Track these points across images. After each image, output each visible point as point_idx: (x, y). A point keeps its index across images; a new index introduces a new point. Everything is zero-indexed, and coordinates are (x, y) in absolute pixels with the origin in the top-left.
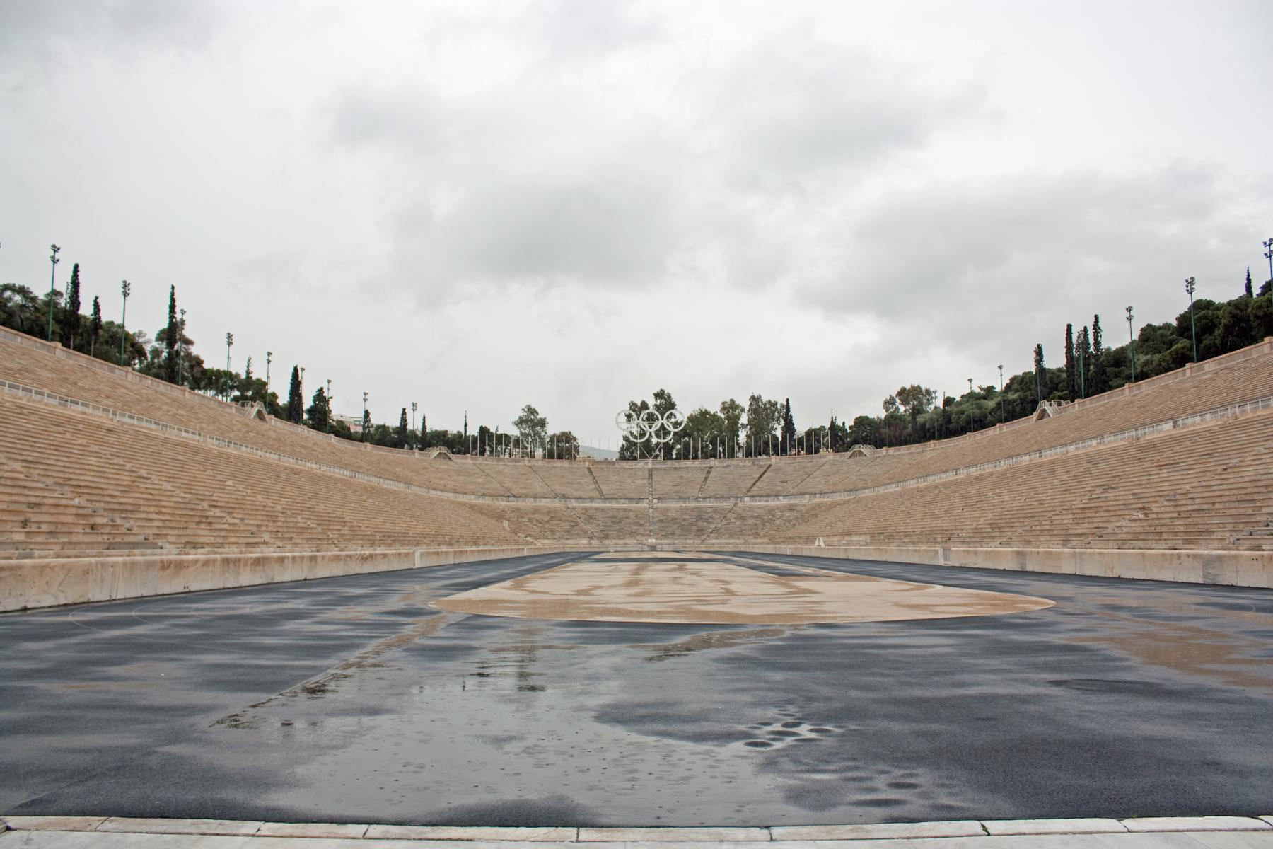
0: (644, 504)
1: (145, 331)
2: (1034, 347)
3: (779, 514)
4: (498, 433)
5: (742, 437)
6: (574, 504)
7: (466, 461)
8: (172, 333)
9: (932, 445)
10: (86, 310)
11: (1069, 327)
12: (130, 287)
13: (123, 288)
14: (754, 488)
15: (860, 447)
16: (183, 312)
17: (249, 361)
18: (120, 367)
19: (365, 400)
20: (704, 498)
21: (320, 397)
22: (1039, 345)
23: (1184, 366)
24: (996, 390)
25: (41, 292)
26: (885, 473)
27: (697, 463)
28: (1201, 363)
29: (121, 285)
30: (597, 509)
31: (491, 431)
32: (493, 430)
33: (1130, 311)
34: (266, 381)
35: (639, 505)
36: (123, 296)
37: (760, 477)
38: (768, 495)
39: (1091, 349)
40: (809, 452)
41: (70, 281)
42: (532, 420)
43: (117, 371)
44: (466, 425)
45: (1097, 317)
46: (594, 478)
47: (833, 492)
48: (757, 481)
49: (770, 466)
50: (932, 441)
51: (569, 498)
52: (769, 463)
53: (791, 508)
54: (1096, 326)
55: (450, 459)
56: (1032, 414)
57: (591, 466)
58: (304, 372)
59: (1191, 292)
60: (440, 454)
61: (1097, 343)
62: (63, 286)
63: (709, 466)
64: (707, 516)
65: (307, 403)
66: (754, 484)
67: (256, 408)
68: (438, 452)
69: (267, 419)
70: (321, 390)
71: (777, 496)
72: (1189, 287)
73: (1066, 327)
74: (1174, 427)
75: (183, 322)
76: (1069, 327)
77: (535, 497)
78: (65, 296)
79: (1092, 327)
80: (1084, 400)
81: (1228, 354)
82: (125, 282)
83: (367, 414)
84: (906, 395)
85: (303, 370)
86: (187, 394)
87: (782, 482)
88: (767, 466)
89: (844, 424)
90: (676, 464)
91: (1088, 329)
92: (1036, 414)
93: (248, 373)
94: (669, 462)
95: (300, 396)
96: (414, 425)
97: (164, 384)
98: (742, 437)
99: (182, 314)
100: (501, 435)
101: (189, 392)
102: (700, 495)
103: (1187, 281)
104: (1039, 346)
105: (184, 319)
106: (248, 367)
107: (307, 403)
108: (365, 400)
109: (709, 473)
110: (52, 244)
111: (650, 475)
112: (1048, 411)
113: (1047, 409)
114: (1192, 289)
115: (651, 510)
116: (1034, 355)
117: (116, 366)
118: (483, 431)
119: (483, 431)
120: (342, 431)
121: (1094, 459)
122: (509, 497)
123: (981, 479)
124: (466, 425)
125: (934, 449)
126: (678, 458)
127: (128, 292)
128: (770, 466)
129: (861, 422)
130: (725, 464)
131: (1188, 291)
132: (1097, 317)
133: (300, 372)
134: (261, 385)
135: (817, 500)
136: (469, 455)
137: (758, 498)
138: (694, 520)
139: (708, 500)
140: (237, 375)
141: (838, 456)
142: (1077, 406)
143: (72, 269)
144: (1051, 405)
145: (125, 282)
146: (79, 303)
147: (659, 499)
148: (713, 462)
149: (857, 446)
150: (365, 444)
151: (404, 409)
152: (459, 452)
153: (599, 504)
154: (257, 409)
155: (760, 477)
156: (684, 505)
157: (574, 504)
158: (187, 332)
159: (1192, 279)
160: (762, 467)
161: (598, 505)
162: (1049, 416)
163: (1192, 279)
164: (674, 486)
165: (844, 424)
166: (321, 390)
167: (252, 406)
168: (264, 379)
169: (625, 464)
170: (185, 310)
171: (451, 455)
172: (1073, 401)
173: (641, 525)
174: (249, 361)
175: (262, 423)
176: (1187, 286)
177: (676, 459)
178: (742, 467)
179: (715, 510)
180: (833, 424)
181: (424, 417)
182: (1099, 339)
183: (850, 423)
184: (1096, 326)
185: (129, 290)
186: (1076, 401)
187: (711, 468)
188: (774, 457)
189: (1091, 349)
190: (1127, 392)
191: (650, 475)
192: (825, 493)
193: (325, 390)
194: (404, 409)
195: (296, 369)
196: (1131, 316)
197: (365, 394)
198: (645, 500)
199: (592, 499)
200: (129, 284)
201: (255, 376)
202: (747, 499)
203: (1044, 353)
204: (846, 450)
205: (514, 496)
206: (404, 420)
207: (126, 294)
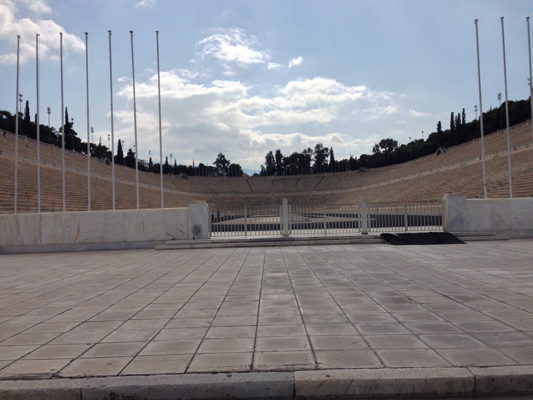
0: (271, 195)
1: (55, 128)
2: (437, 123)
3: (328, 197)
4: (208, 166)
5: (312, 163)
6: (241, 195)
7: (195, 179)
8: (68, 127)
9: (394, 166)
10: (32, 120)
11: (452, 114)
12: (51, 110)
13: (48, 110)
14: (318, 186)
15: (362, 168)
16: (72, 119)
17: (100, 138)
18: (50, 145)
19: (150, 153)
20: (296, 192)
21: (131, 153)
22: (440, 122)
23: (497, 131)
24: (425, 141)
25: (13, 113)
26: (373, 179)
27: (293, 176)
28: (503, 130)
29: (47, 109)
30: (251, 197)
31: (204, 165)
32: (205, 165)
33: (476, 107)
34: (108, 148)
35: (269, 195)
36: (48, 114)
37: (320, 182)
38: (323, 190)
39: (461, 123)
40: (341, 171)
41: (25, 108)
42: (222, 160)
43: (48, 146)
44: (194, 163)
45: (464, 109)
46: (249, 184)
47: (351, 187)
48: (319, 184)
49: (324, 177)
50: (394, 165)
51: (239, 193)
52: (324, 176)
53: (332, 195)
54: (463, 113)
55: (187, 178)
56: (435, 152)
57: (248, 179)
58: (124, 143)
59: (500, 99)
60: (183, 176)
61: (464, 121)
62: (23, 112)
63: (298, 177)
64: (297, 199)
65: (125, 155)
66: (317, 185)
67: (105, 159)
68: (182, 175)
69: (110, 164)
70: (130, 150)
71: (327, 189)
72: (499, 97)
73: (451, 114)
74: (480, 159)
75: (72, 123)
76: (452, 114)
77: (224, 193)
78: (24, 115)
79: (462, 114)
80: (457, 146)
81: (513, 126)
82: (48, 108)
83: (151, 159)
84: (384, 143)
85: (123, 141)
86: (77, 154)
87: (329, 184)
88: (323, 177)
89: (356, 158)
90: (284, 177)
91: (460, 114)
92: (436, 153)
93: (100, 143)
94: (281, 177)
95: (122, 152)
96: (171, 163)
97: (67, 151)
98: (312, 163)
99: (72, 120)
100: (209, 166)
101: (78, 154)
102: (294, 190)
103: (498, 95)
104: (440, 122)
105: (73, 122)
106: (100, 141)
107: (125, 155)
108: (150, 153)
109: (298, 181)
110: (48, 107)
111: (273, 182)
112: (442, 151)
113: (441, 150)
114: (500, 98)
115: (274, 198)
116: (437, 127)
117: (48, 144)
118: (201, 165)
119: (201, 165)
120: (141, 167)
121: (446, 173)
122: (213, 193)
123: (407, 181)
124: (194, 163)
125: (395, 169)
126: (285, 175)
127: (50, 112)
128: (324, 177)
129: (363, 157)
130: (305, 177)
131: (498, 99)
132: (464, 109)
133: (121, 142)
134: (105, 148)
135: (344, 191)
136: (195, 176)
137: (319, 191)
138: (292, 201)
139: (298, 192)
140: (95, 145)
141: (353, 172)
142: (453, 149)
143: (26, 103)
144: (442, 148)
145: (48, 108)
146: (30, 117)
147: (277, 192)
148: (299, 176)
149: (362, 167)
150: (151, 173)
151: (167, 157)
152: (191, 175)
153: (251, 195)
154: (106, 160)
155: (320, 182)
156: (288, 195)
157: (241, 195)
158: (74, 128)
159: (500, 94)
160: (320, 177)
161: (251, 196)
162: (442, 153)
163: (500, 94)
164: (283, 186)
165: (356, 158)
166: (130, 150)
167: (104, 158)
168: (107, 146)
169: (262, 178)
170: (73, 118)
171: (188, 176)
172: (452, 147)
173: (269, 204)
174: (100, 138)
175: (108, 166)
176: (498, 97)
177: (284, 175)
178: (313, 178)
179: (301, 196)
180: (351, 158)
181: (175, 161)
182: (465, 119)
183: (358, 158)
184: (463, 113)
185: (50, 111)
186: (453, 146)
187: (299, 178)
188: (326, 173)
189: (461, 123)
190: (474, 142)
191: (273, 182)
192: (347, 188)
193: (133, 149)
194: (167, 157)
195: (120, 141)
196: (476, 110)
197: (150, 151)
198: (271, 193)
199: (248, 193)
200: (50, 109)
201: (102, 145)
202: (314, 192)
203: (442, 125)
204: (357, 170)
205: (216, 193)
206: (167, 162)
207: (49, 113)
